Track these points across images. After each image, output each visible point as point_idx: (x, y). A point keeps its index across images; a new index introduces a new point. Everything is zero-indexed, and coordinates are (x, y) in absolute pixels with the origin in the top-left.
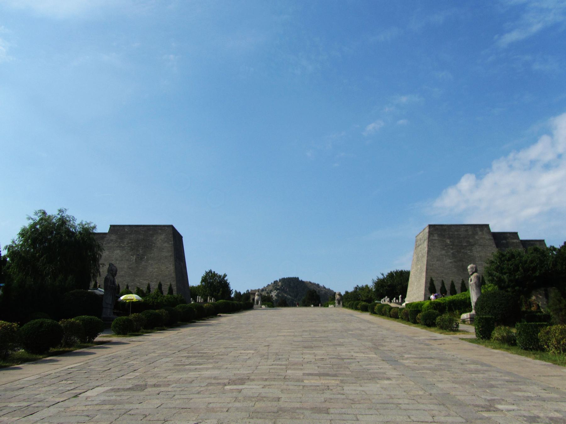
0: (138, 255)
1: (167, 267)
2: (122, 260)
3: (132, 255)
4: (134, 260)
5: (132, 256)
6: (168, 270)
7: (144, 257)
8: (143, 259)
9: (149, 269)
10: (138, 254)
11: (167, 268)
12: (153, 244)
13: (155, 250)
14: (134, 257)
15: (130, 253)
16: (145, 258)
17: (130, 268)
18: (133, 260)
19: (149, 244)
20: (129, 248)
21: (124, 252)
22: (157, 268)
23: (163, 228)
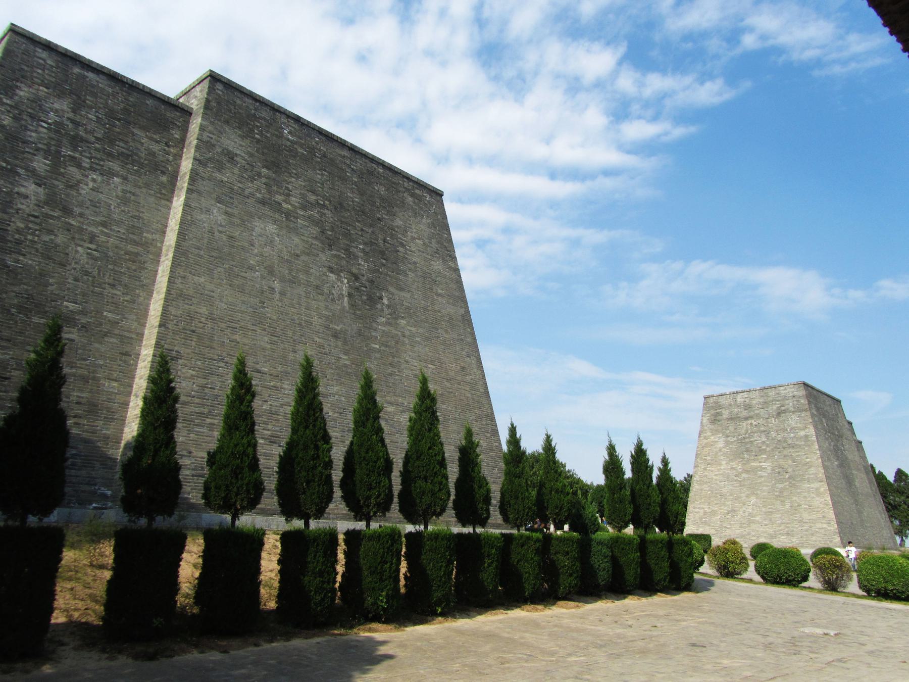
0: (356, 278)
1: (462, 364)
2: (293, 281)
3: (331, 269)
4: (346, 299)
5: (332, 276)
6: (468, 378)
7: (381, 298)
8: (379, 306)
9: (408, 358)
10: (354, 270)
11: (463, 368)
12: (401, 249)
13: (411, 275)
14: (342, 282)
15: (323, 257)
16: (385, 301)
17: (336, 336)
18: (343, 297)
19: (385, 241)
20: (315, 230)
21: (296, 240)
22: (432, 362)
23: (417, 192)
